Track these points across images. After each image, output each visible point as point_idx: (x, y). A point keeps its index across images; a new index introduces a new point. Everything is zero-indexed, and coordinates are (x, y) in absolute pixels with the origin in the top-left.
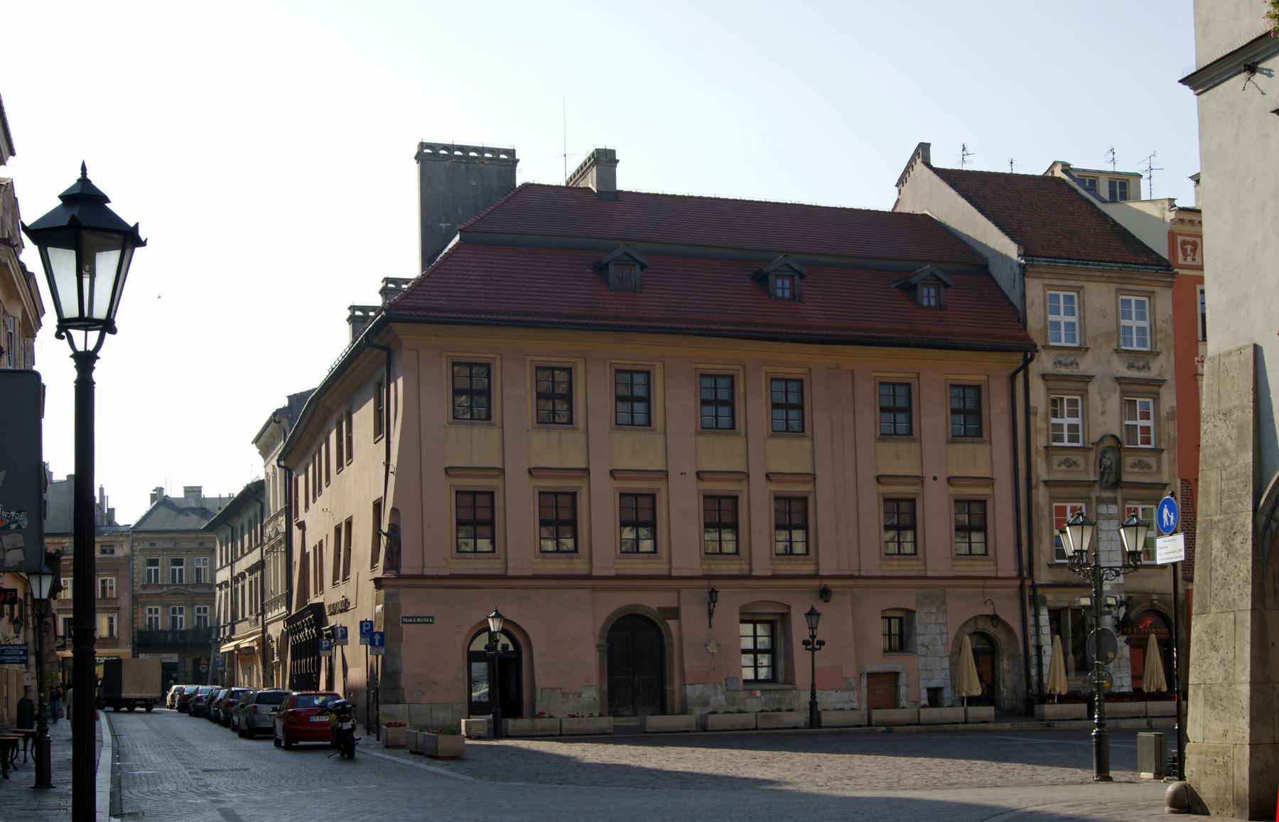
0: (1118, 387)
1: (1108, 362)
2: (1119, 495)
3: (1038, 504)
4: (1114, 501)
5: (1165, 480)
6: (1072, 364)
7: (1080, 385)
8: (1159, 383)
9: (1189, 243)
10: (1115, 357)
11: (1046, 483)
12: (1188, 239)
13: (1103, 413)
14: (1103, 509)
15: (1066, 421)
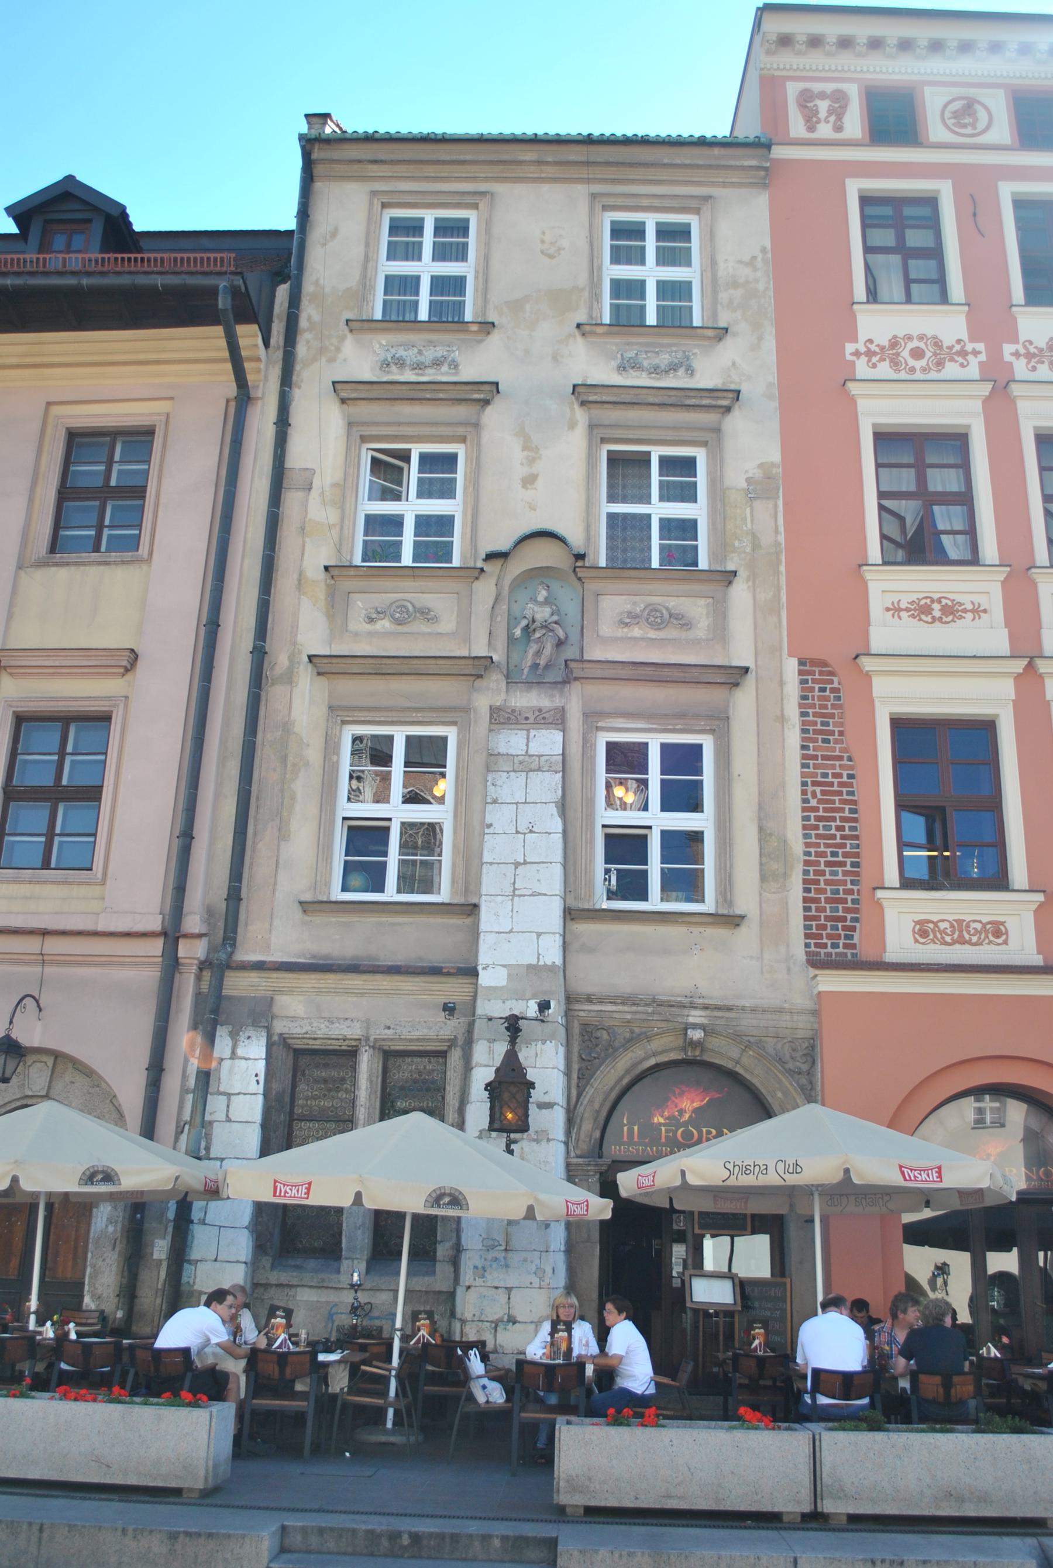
0: (581, 416)
1: (556, 358)
2: (574, 702)
3: (287, 727)
4: (558, 720)
5: (741, 655)
6: (437, 363)
7: (461, 412)
8: (725, 400)
9: (822, 95)
10: (579, 346)
11: (323, 665)
12: (817, 87)
13: (529, 481)
14: (512, 742)
15: (412, 507)
